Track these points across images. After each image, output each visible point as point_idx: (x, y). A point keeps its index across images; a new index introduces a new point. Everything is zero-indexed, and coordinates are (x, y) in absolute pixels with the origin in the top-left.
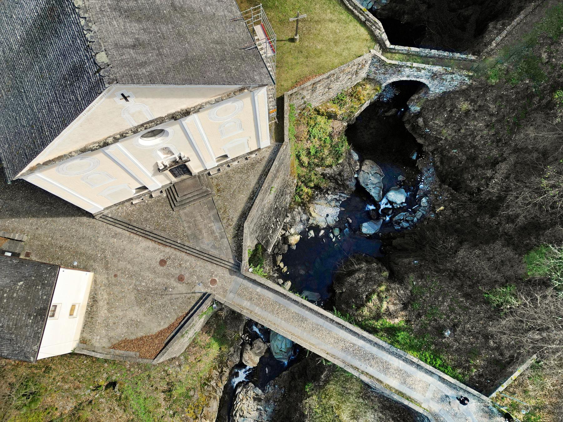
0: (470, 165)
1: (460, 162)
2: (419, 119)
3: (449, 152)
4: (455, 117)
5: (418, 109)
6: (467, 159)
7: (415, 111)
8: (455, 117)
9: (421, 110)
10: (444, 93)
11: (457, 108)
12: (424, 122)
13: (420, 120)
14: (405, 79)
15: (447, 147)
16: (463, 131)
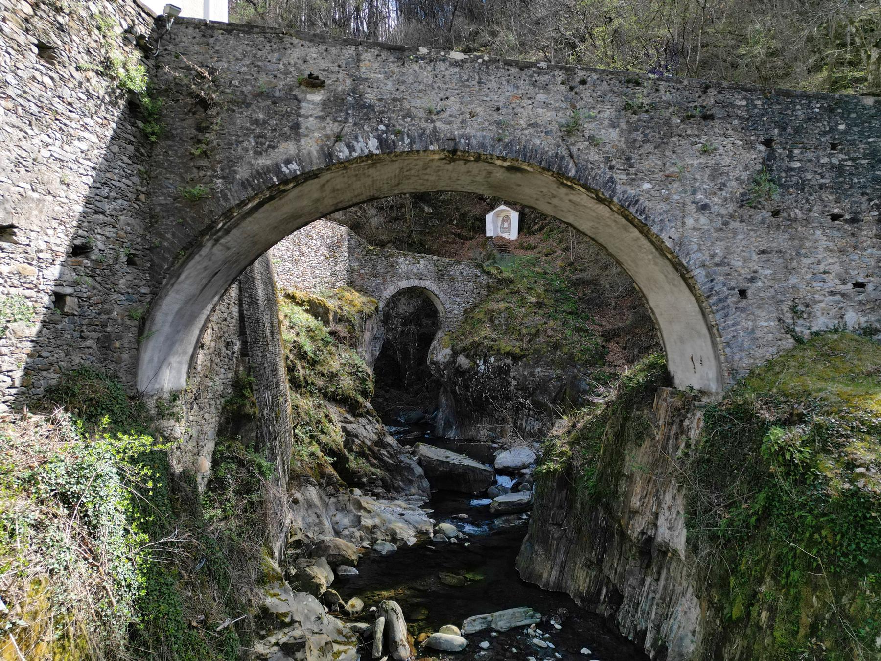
0: (575, 370)
1: (559, 378)
2: (458, 359)
3: (534, 376)
4: (500, 324)
5: (448, 351)
6: (563, 369)
7: (445, 357)
8: (500, 324)
9: (452, 349)
10: (465, 312)
11: (493, 311)
12: (467, 357)
13: (462, 360)
14: (404, 284)
15: (526, 373)
16: (524, 331)
